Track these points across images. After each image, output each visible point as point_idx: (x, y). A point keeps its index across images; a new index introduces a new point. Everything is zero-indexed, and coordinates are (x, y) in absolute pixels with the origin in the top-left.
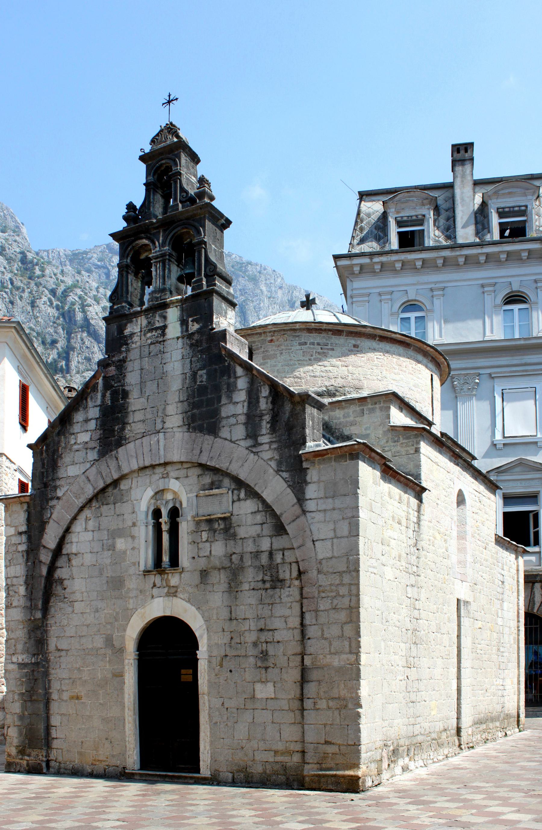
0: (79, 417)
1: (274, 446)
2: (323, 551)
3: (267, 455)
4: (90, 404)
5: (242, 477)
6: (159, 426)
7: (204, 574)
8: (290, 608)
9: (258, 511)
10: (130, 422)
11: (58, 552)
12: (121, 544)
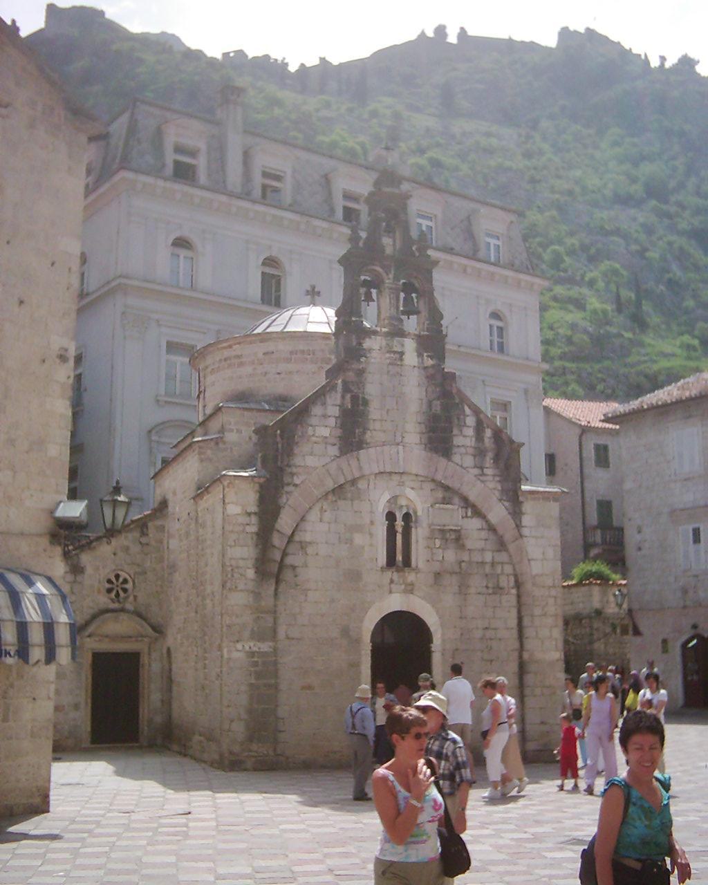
0: (317, 410)
1: (498, 479)
2: (536, 568)
3: (491, 485)
4: (329, 401)
5: (472, 498)
6: (399, 439)
7: (438, 575)
8: (509, 612)
9: (482, 529)
10: (371, 428)
11: (290, 539)
12: (359, 539)
